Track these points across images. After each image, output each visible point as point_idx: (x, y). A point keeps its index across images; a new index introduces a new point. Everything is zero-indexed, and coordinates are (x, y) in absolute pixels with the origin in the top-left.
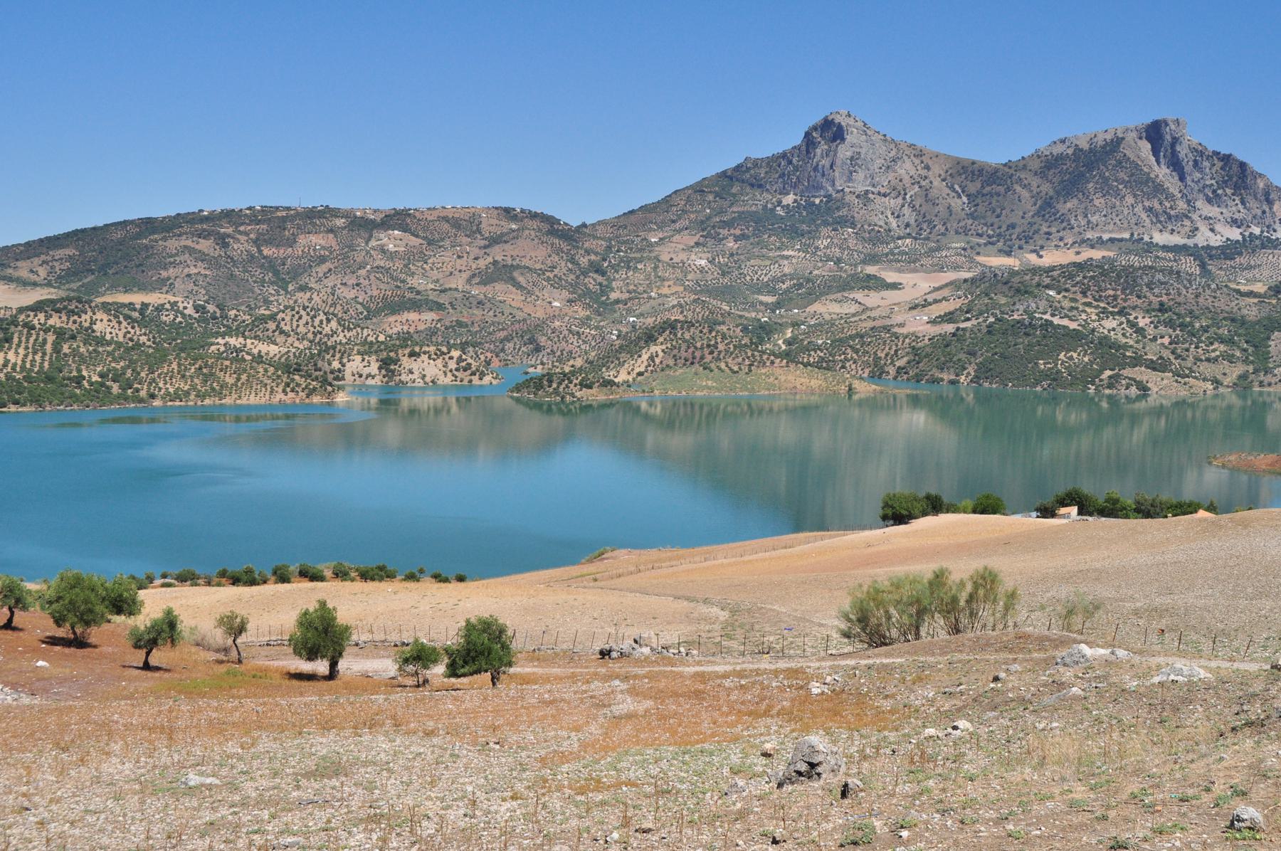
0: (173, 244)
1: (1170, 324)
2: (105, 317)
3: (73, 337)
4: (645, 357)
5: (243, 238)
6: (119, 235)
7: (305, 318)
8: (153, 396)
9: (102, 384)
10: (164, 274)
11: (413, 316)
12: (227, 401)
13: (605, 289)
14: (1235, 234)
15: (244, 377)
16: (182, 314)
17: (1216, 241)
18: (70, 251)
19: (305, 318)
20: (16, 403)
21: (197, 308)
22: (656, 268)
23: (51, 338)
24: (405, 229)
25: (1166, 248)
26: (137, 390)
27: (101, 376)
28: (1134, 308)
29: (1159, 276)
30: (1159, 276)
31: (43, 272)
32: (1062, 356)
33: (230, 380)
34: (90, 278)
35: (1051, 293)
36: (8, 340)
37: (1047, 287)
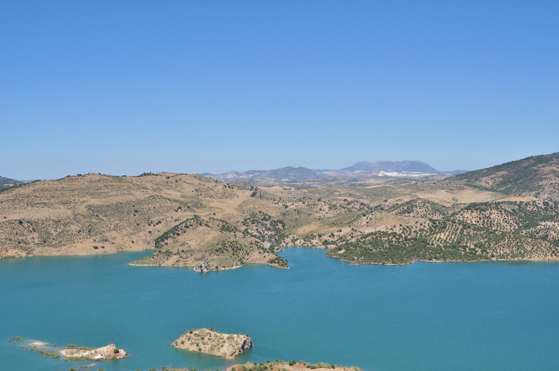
0: (547, 169)
2: (496, 212)
3: (469, 227)
6: (525, 164)
8: (493, 256)
9: (474, 250)
10: (541, 183)
12: (525, 259)
15: (535, 247)
16: (537, 207)
18: (504, 173)
20: (436, 258)
21: (545, 203)
23: (461, 227)
26: (488, 253)
27: (475, 245)
31: (491, 183)
33: (529, 249)
34: (510, 185)
36: (445, 227)
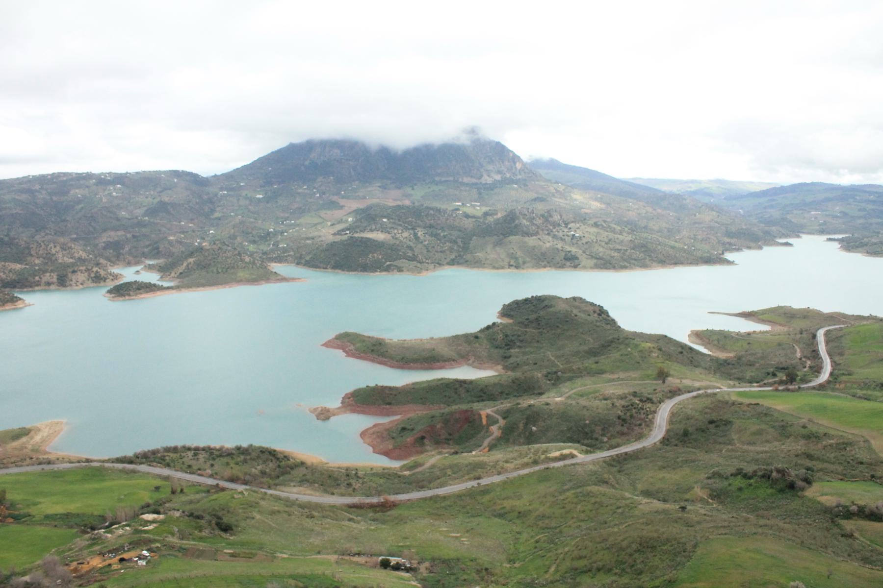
1: (431, 235)
4: (185, 264)
5: (44, 192)
7: (43, 246)
11: (112, 233)
13: (213, 211)
14: (498, 177)
17: (489, 181)
19: (43, 246)
22: (238, 200)
24: (123, 184)
25: (467, 185)
28: (419, 226)
29: (432, 212)
30: (432, 212)
32: (370, 256)
35: (385, 220)
37: (385, 217)
